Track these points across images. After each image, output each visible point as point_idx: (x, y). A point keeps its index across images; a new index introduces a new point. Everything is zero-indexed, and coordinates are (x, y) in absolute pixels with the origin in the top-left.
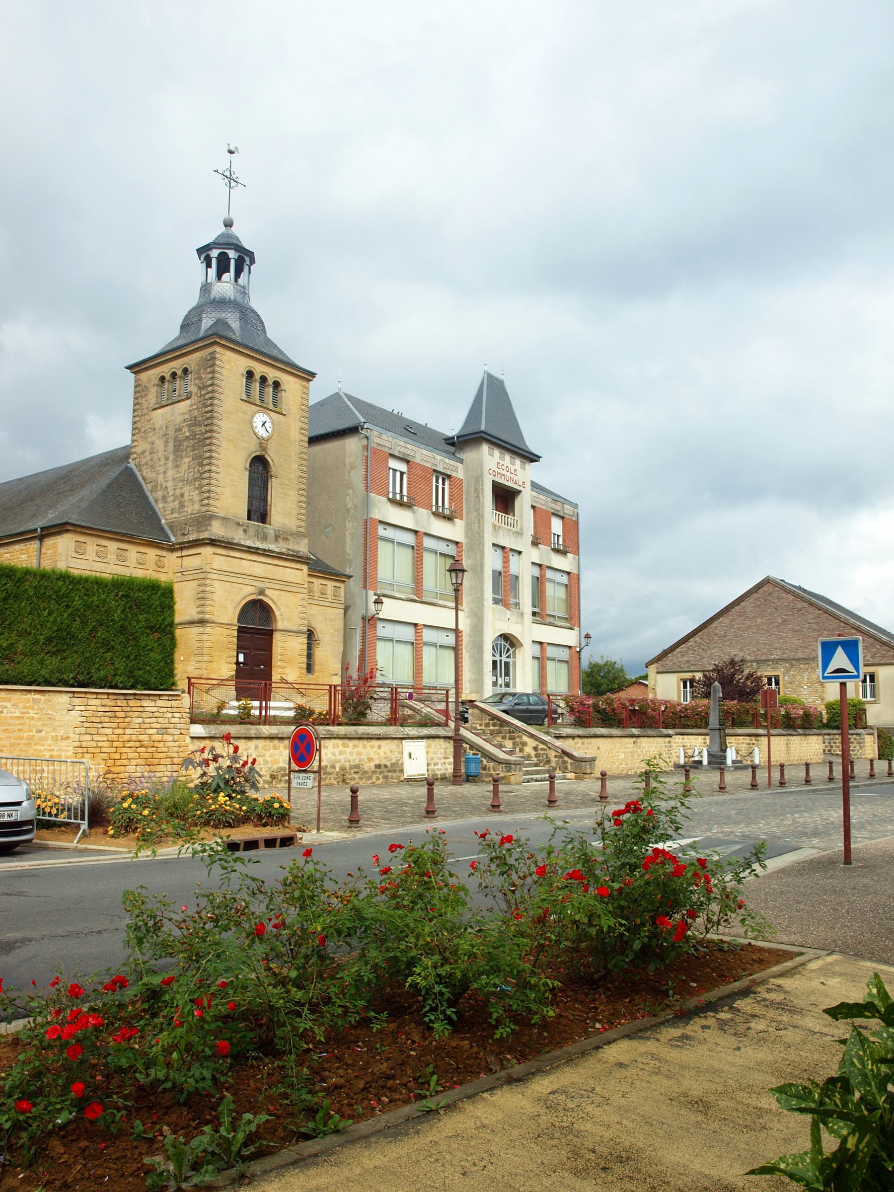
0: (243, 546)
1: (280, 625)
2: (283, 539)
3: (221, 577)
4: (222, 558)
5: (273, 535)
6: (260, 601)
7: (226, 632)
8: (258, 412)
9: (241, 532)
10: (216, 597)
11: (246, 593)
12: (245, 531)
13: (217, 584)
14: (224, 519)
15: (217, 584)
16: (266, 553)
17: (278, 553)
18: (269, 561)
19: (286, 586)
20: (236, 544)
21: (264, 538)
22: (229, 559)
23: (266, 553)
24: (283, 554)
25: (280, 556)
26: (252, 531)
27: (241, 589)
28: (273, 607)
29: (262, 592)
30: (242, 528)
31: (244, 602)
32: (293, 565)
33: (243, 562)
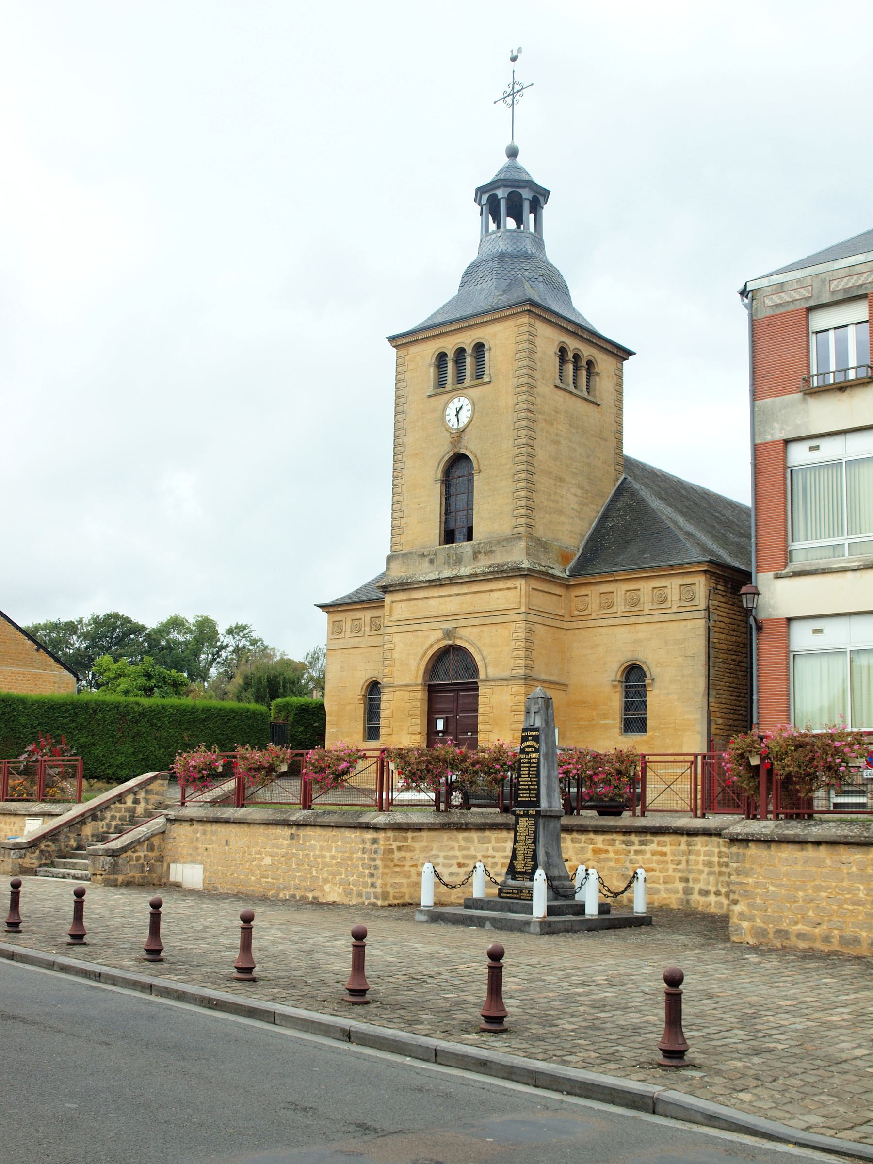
0: (421, 582)
1: (482, 675)
2: (485, 554)
3: (401, 629)
4: (404, 604)
5: (470, 553)
6: (450, 646)
7: (407, 695)
8: (451, 399)
9: (426, 564)
10: (396, 655)
11: (432, 640)
12: (431, 561)
13: (397, 638)
14: (404, 555)
15: (397, 638)
16: (453, 581)
17: (468, 576)
18: (464, 589)
19: (490, 618)
20: (412, 583)
21: (459, 561)
22: (412, 603)
23: (453, 581)
24: (476, 575)
25: (473, 579)
26: (441, 559)
27: (428, 637)
28: (472, 650)
29: (448, 634)
30: (427, 559)
31: (430, 653)
32: (501, 584)
33: (432, 602)
